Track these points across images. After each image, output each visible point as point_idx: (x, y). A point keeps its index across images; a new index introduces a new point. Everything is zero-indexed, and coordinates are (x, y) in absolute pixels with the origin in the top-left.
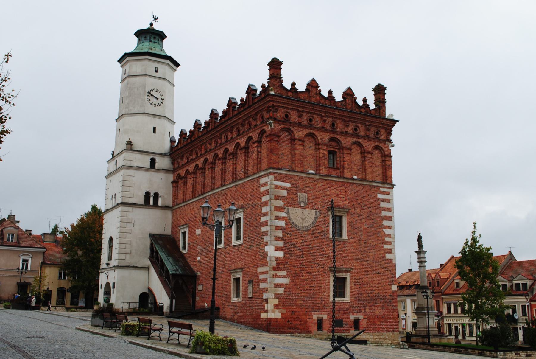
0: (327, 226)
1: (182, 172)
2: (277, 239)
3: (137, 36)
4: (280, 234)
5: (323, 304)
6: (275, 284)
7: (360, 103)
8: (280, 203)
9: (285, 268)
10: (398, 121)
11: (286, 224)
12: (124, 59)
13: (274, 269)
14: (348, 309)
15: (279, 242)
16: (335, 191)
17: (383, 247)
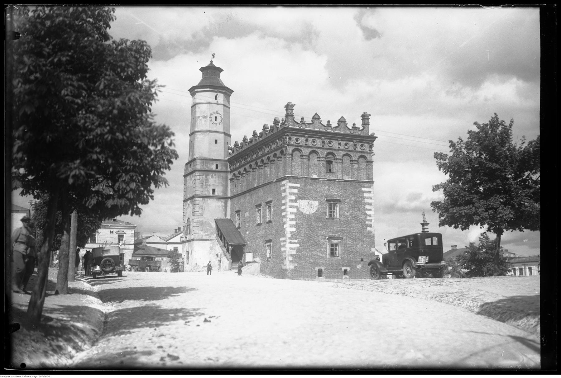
1: (236, 172)
2: (292, 220)
3: (202, 71)
4: (293, 216)
7: (350, 126)
8: (293, 198)
10: (377, 137)
12: (193, 91)
13: (289, 238)
17: (365, 223)
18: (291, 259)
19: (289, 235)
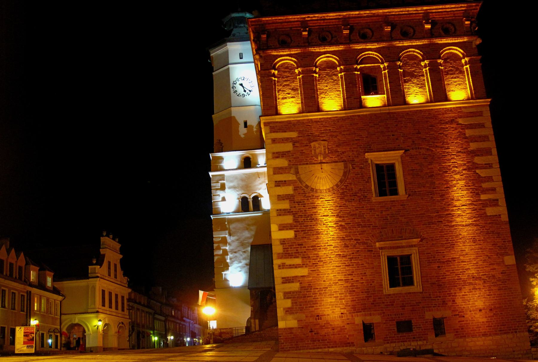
0: (366, 182)
4: (285, 205)
5: (371, 300)
6: (283, 278)
9: (299, 252)
11: (294, 190)
13: (280, 256)
14: (421, 303)
15: (285, 217)
16: (378, 128)
18: (288, 303)
19: (277, 249)
